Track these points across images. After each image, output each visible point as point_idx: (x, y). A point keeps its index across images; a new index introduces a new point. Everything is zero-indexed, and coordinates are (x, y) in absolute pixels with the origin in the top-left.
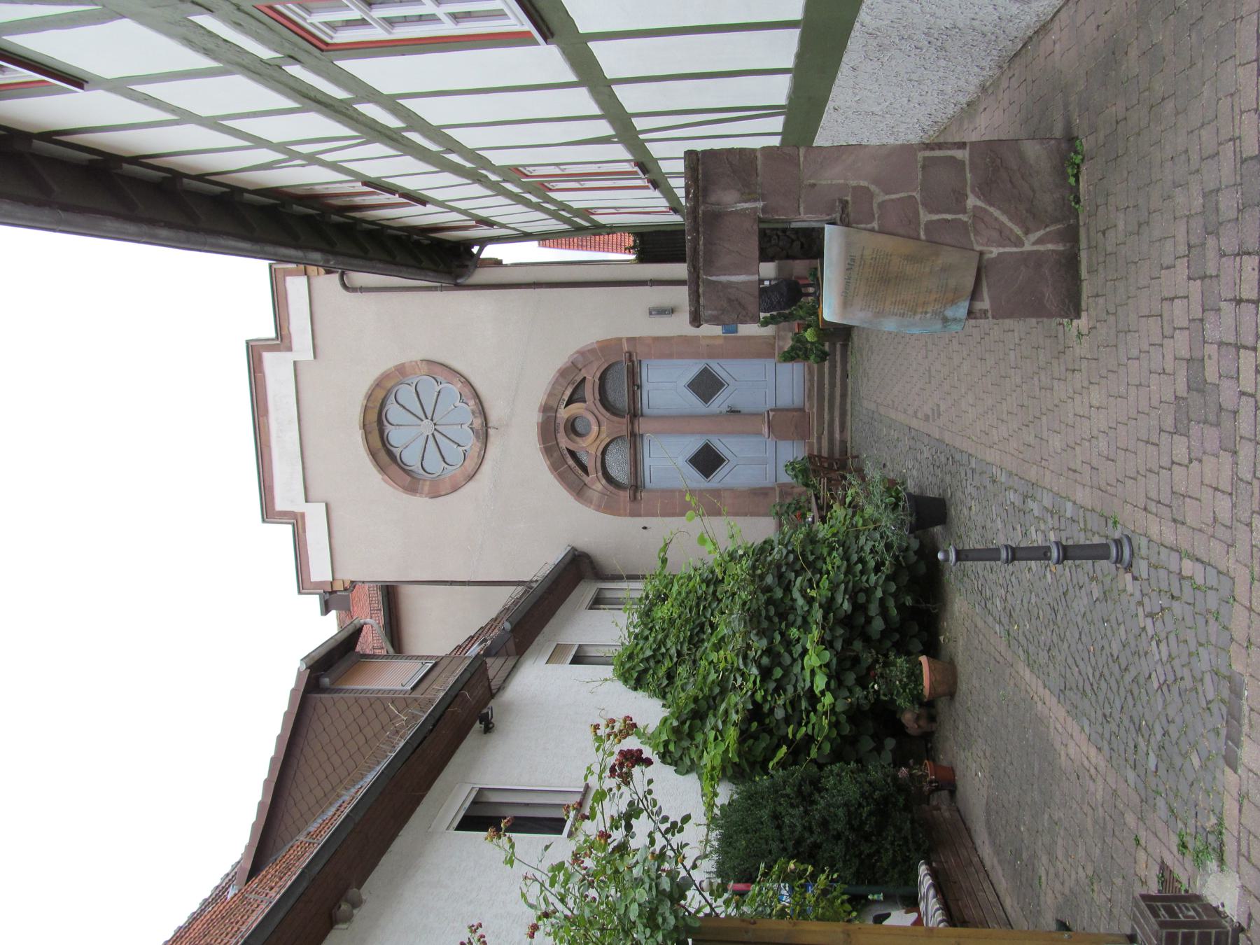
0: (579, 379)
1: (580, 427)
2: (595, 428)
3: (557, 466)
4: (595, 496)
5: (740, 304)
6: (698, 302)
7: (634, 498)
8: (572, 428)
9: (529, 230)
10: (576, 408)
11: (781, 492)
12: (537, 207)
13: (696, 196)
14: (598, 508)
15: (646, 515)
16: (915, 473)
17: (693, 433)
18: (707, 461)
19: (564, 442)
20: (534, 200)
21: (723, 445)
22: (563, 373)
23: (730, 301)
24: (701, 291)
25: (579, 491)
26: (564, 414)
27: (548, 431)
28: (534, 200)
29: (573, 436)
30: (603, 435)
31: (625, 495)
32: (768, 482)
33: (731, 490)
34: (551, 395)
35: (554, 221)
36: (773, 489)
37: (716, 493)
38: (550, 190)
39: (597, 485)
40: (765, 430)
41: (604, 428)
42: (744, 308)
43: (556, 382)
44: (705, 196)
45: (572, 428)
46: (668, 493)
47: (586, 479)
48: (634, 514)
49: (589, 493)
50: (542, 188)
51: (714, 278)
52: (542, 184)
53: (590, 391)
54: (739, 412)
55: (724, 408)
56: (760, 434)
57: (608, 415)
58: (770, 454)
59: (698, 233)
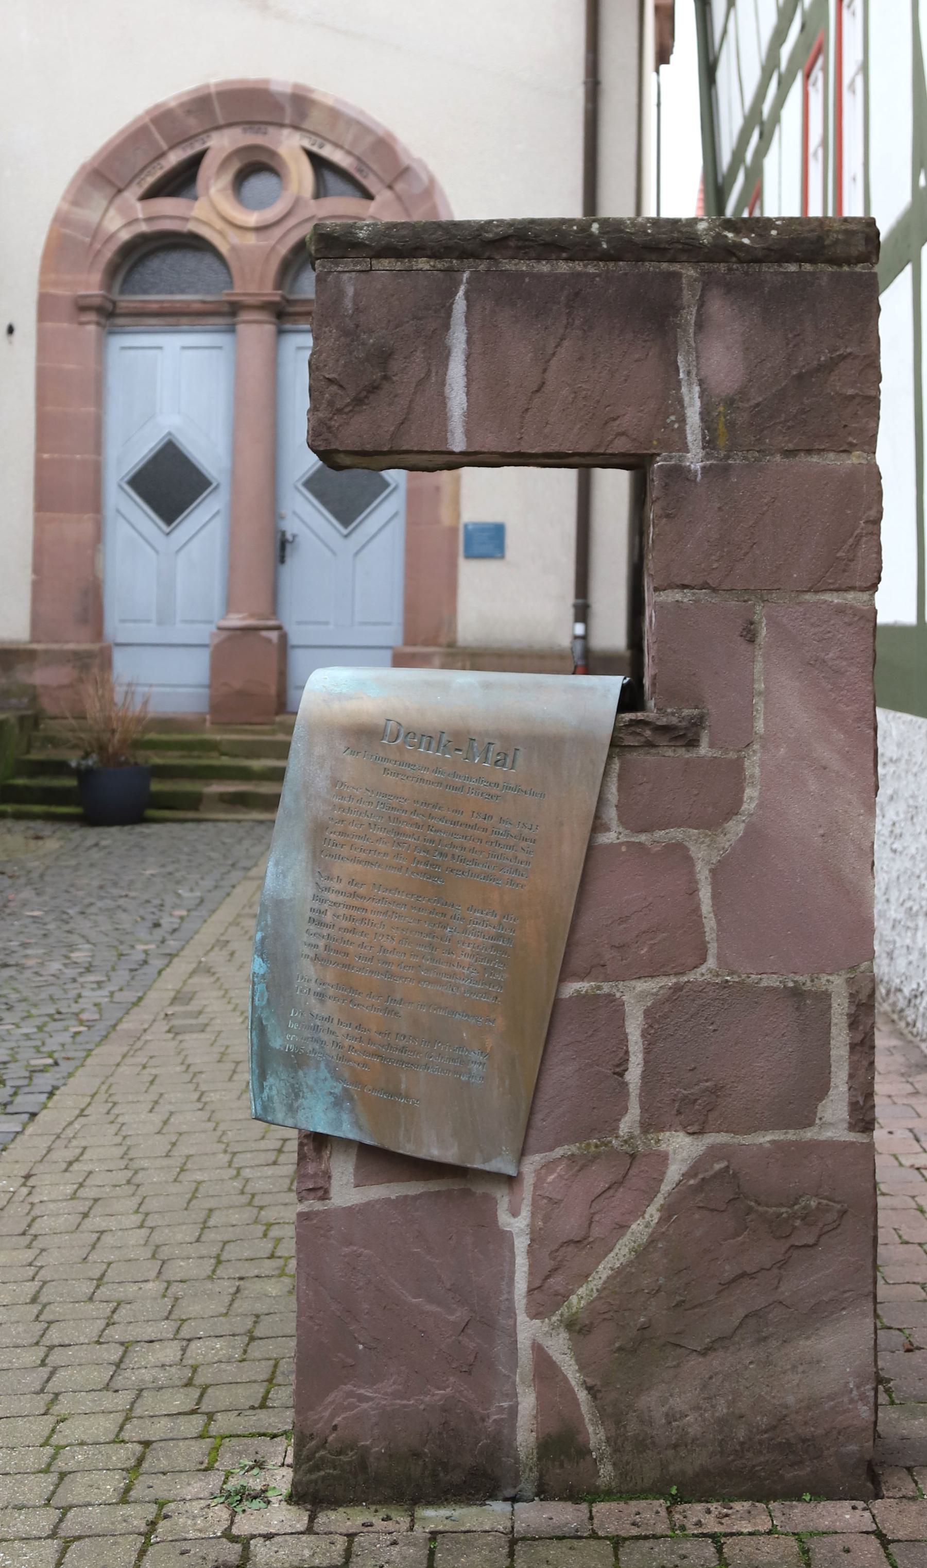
0: (370, 183)
1: (258, 184)
2: (252, 219)
3: (164, 123)
4: (91, 214)
5: (374, 388)
6: (380, 253)
7: (82, 307)
8: (254, 166)
9: (722, 75)
10: (301, 175)
11: (90, 655)
12: (770, 65)
13: (728, 252)
14: (61, 220)
15: (42, 336)
16: (55, 966)
17: (235, 450)
18: (169, 484)
19: (222, 144)
20: (786, 52)
21: (206, 521)
22: (384, 146)
23: (383, 356)
24: (423, 264)
25: (104, 175)
26: (290, 146)
27: (251, 105)
28: (786, 52)
29: (236, 166)
30: (235, 238)
31: (91, 284)
32: (116, 626)
33: (98, 536)
34: (334, 115)
35: (738, 122)
36: (99, 634)
37: (94, 502)
38: (807, 76)
39: (123, 218)
40: (235, 621)
41: (251, 240)
42: (359, 401)
43: (363, 128)
44: (729, 288)
45: (254, 166)
46: (96, 388)
47: (131, 195)
48: (46, 306)
49: (99, 200)
50: (812, 52)
51: (460, 305)
52: (821, 50)
53: (341, 207)
54: (282, 560)
55: (291, 526)
56: (230, 605)
57: (284, 250)
58: (180, 633)
59: (606, 257)
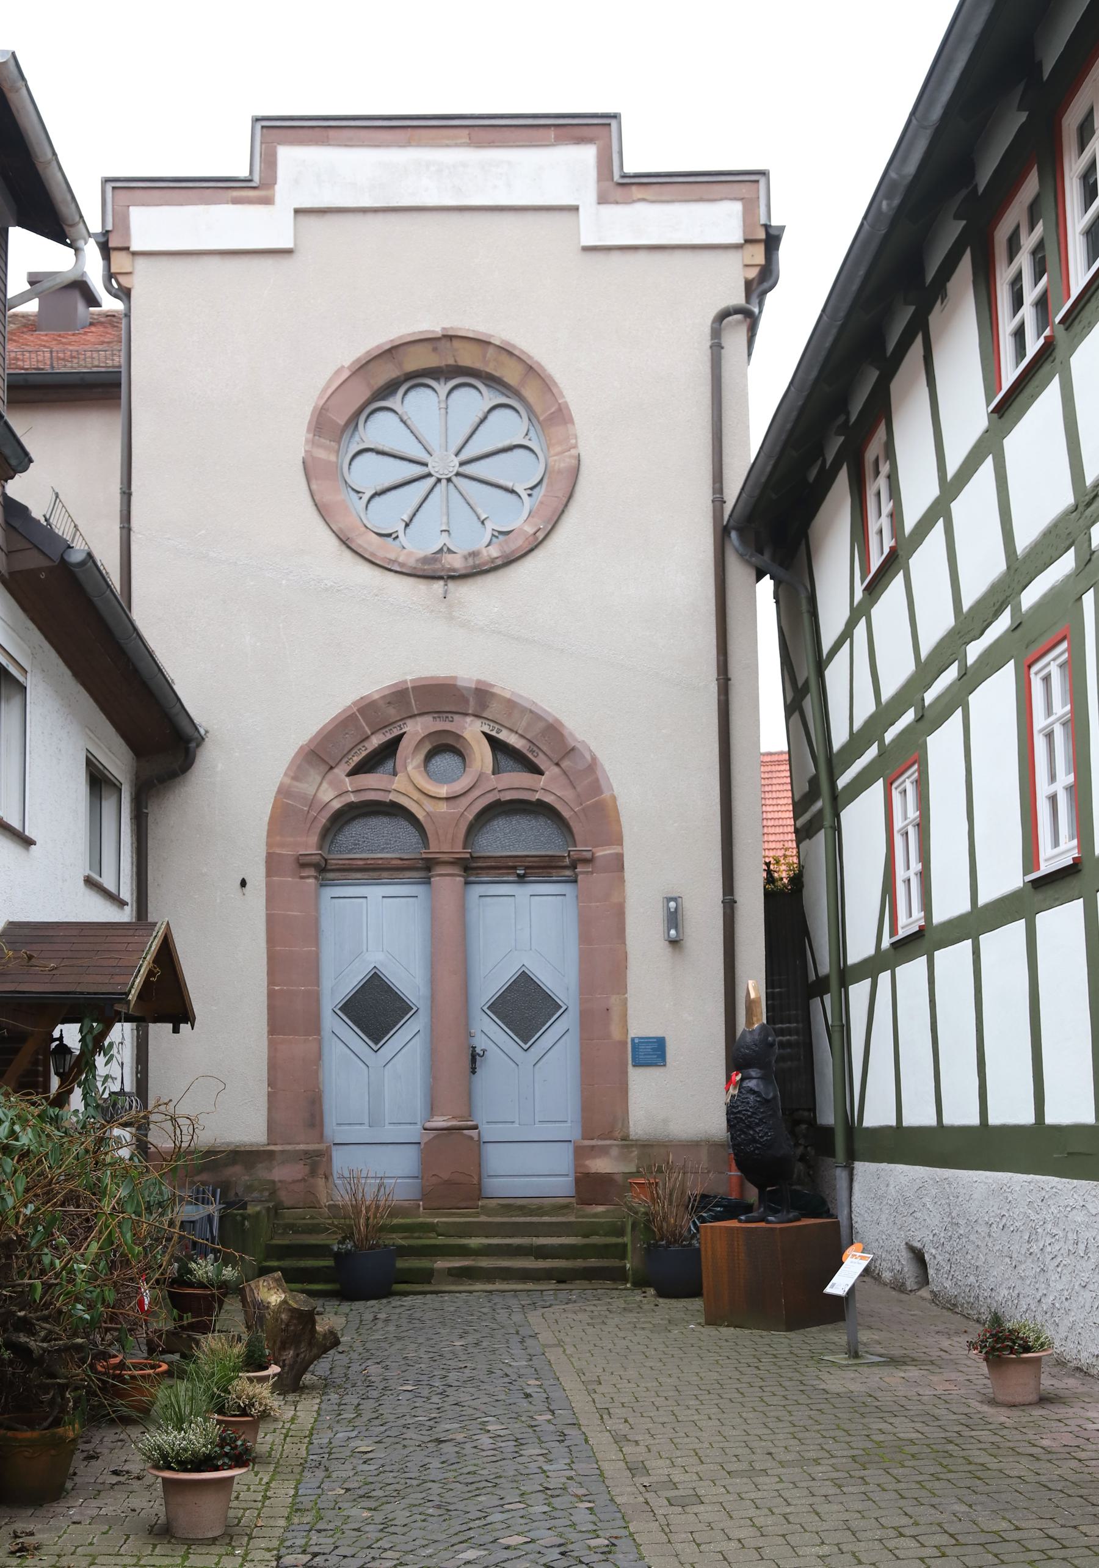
0: (540, 761)
2: (443, 791)
4: (307, 787)
8: (445, 747)
10: (482, 755)
14: (283, 792)
15: (269, 886)
17: (433, 982)
18: (375, 1009)
19: (416, 729)
21: (408, 1042)
22: (553, 731)
25: (318, 755)
26: (472, 731)
27: (440, 698)
29: (428, 747)
30: (430, 806)
31: (309, 845)
32: (335, 1128)
33: (320, 1056)
34: (511, 705)
37: (313, 1026)
39: (332, 791)
40: (440, 1122)
41: (443, 807)
43: (535, 716)
46: (313, 931)
47: (341, 771)
48: (272, 863)
49: (314, 776)
53: (515, 783)
54: (474, 1071)
55: (480, 1043)
56: (433, 1109)
57: (470, 816)
58: (389, 1133)
